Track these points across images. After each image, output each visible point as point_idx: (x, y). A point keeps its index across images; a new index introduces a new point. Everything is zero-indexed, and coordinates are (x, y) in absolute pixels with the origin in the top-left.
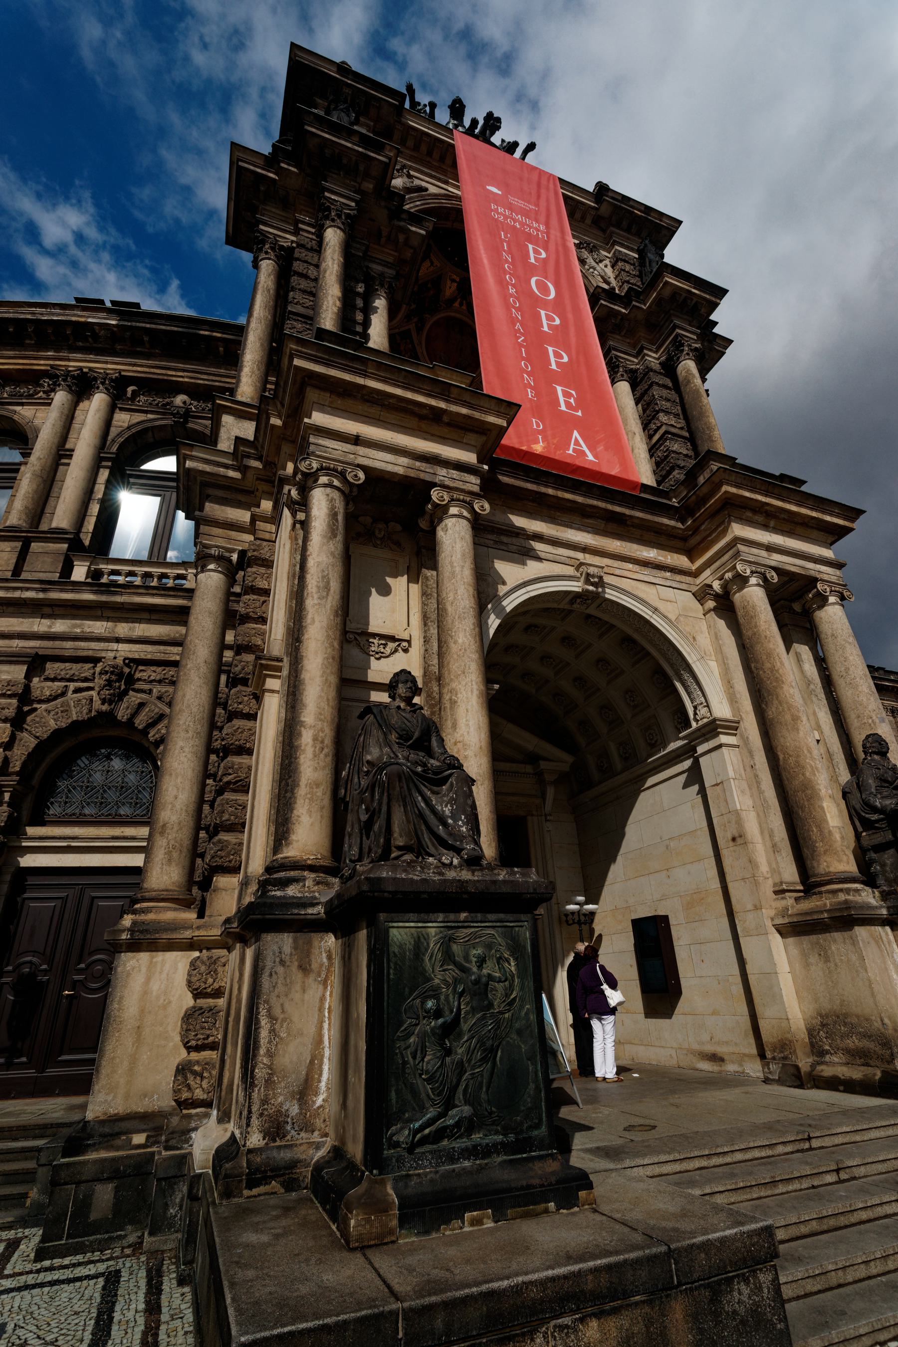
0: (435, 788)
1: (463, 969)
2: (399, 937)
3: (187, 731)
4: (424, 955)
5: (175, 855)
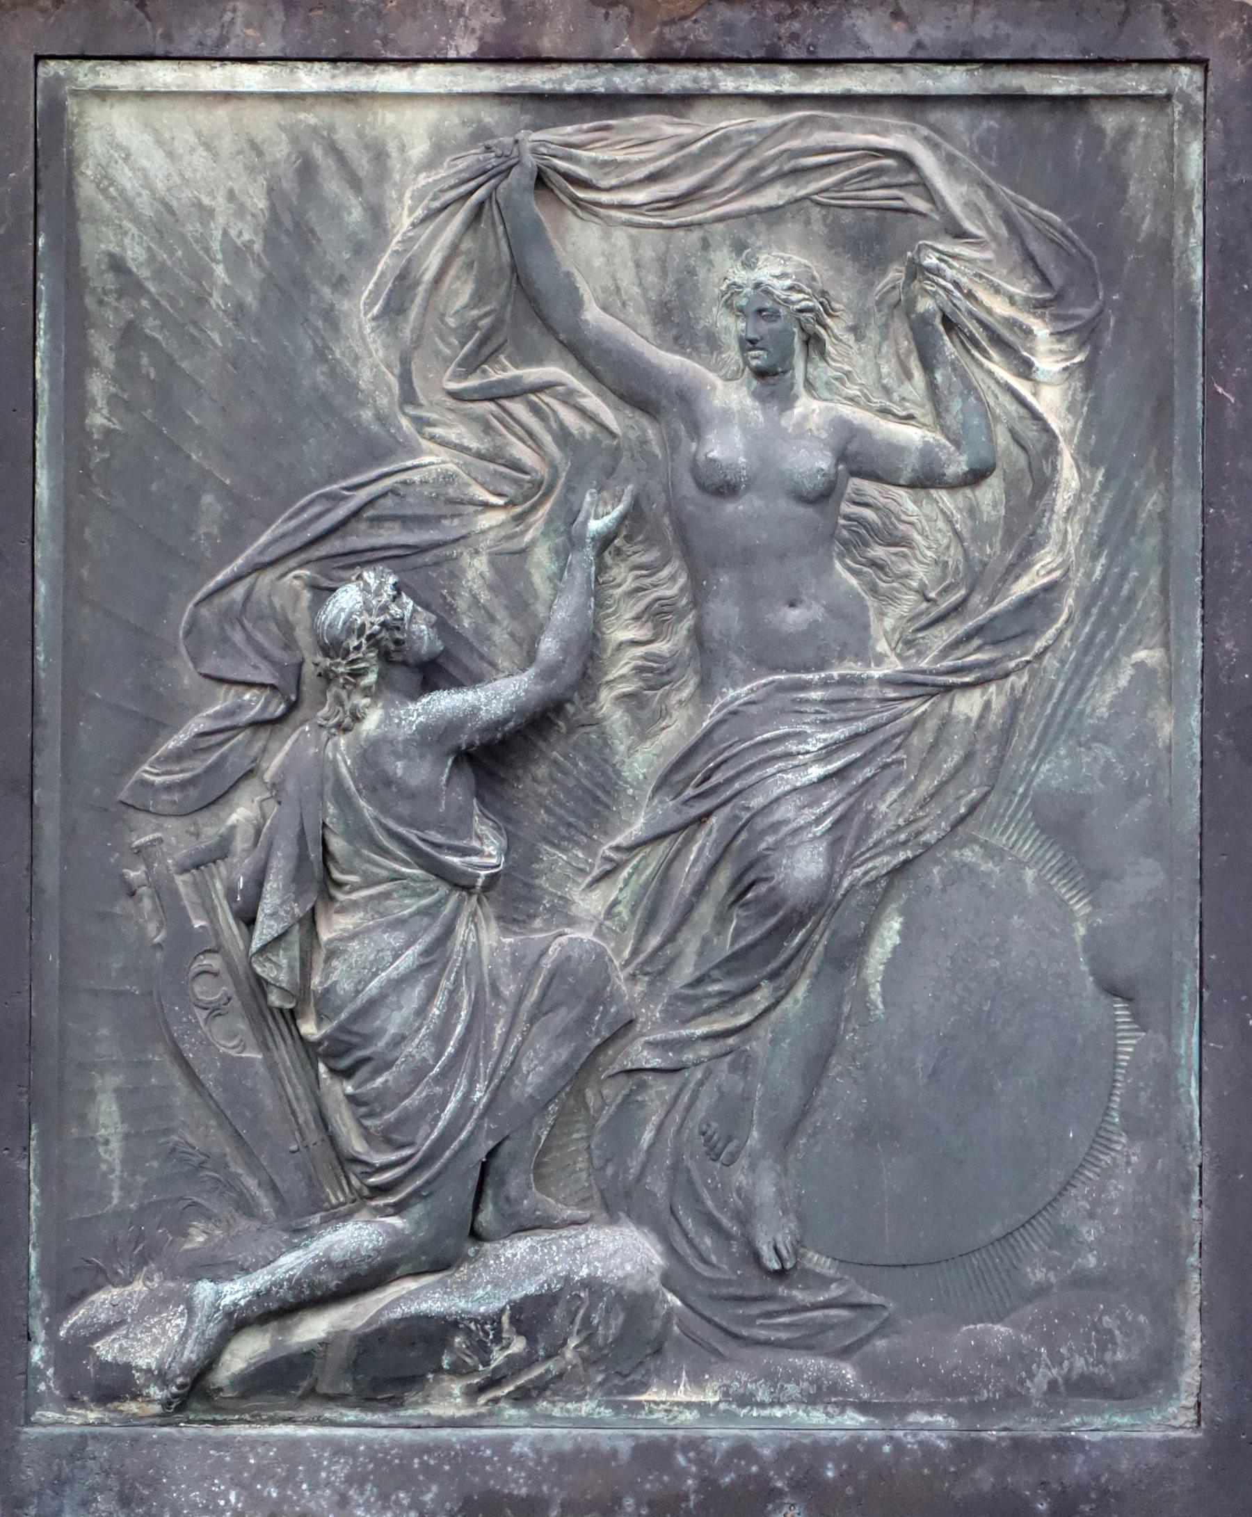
1: (638, 391)
2: (156, 164)
4: (341, 284)
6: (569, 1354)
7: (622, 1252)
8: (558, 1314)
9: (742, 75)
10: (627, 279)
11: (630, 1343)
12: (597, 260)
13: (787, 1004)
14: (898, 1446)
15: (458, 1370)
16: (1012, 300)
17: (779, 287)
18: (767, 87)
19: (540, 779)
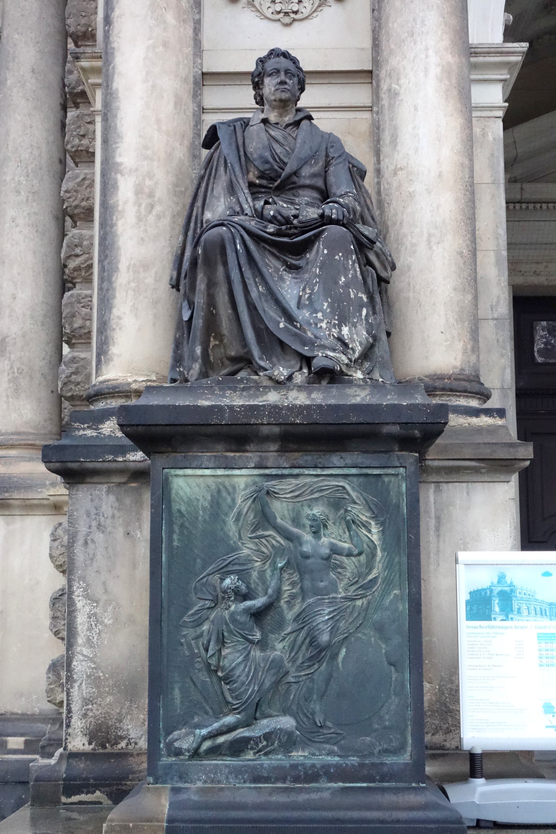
0: (292, 261)
1: (288, 536)
2: (188, 490)
3: (18, 192)
4: (226, 515)
5: (24, 382)
6: (276, 745)
7: (287, 722)
8: (273, 736)
10: (286, 513)
11: (289, 742)
12: (280, 509)
13: (321, 668)
14: (347, 765)
15: (252, 749)
16: (366, 517)
17: (318, 514)
18: (315, 473)
19: (268, 619)
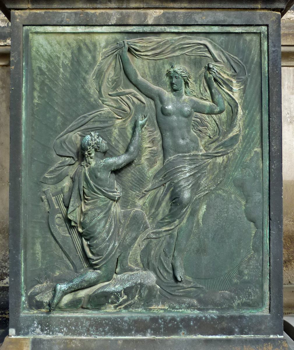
2: (48, 48)
4: (87, 72)
6: (136, 298)
8: (134, 291)
9: (170, 28)
10: (147, 71)
11: (149, 297)
13: (182, 224)
14: (206, 318)
15: (112, 303)
16: (228, 75)
17: (179, 72)
18: (176, 31)
19: (129, 175)
